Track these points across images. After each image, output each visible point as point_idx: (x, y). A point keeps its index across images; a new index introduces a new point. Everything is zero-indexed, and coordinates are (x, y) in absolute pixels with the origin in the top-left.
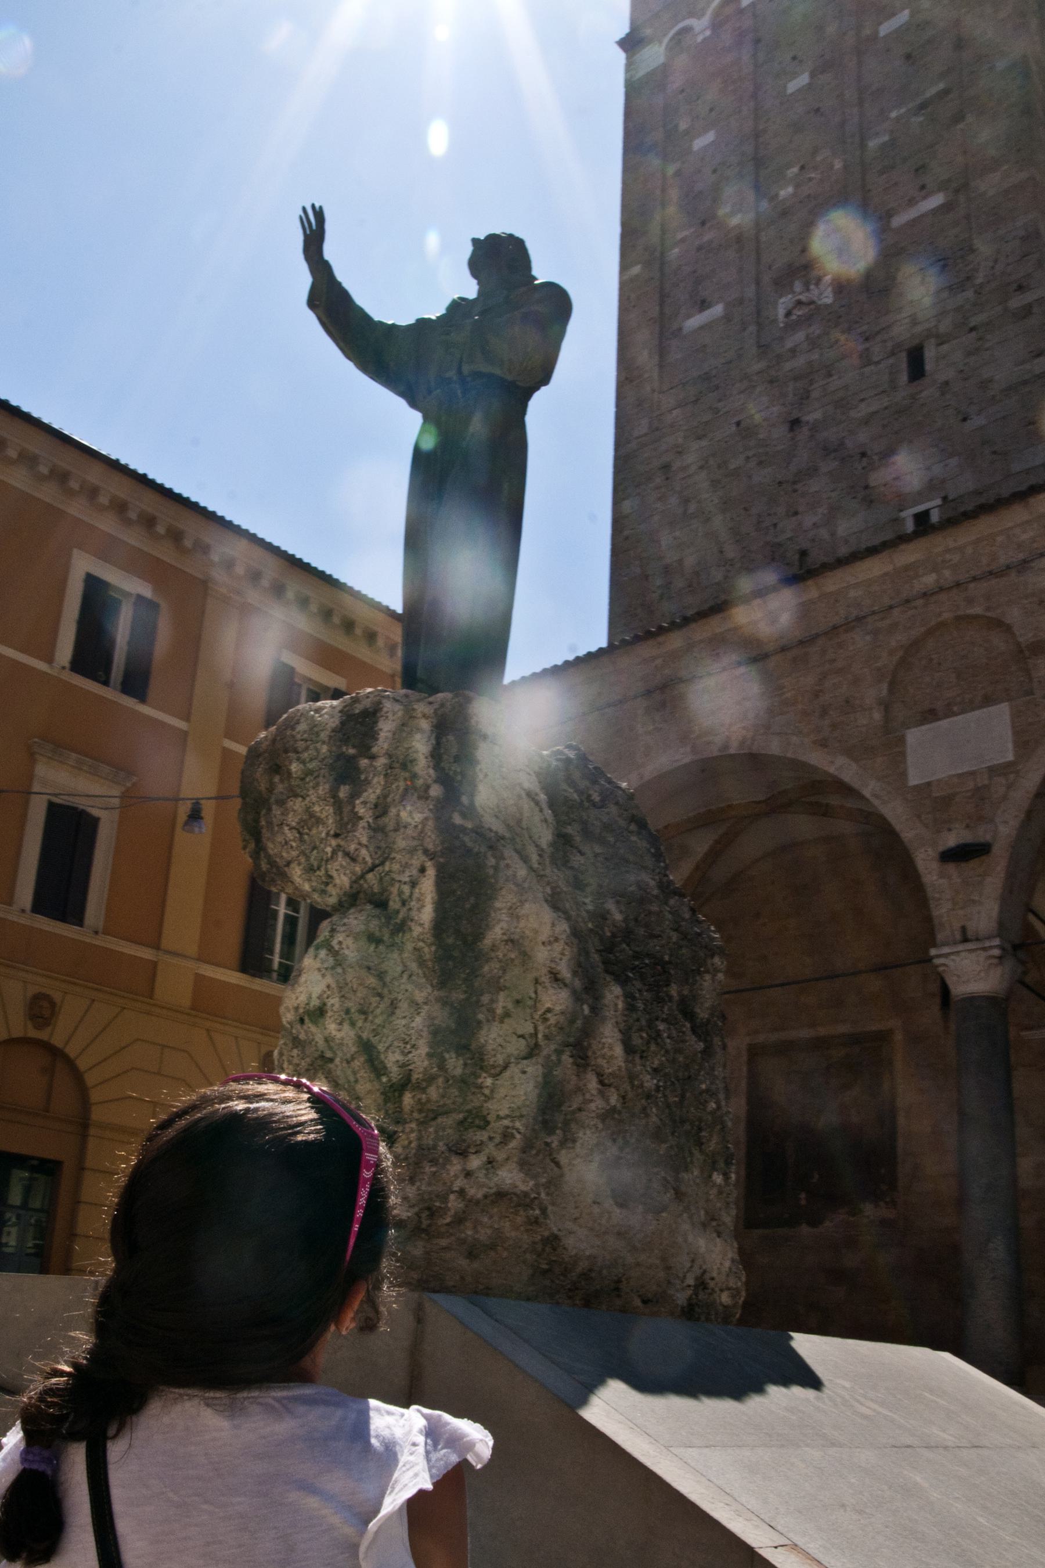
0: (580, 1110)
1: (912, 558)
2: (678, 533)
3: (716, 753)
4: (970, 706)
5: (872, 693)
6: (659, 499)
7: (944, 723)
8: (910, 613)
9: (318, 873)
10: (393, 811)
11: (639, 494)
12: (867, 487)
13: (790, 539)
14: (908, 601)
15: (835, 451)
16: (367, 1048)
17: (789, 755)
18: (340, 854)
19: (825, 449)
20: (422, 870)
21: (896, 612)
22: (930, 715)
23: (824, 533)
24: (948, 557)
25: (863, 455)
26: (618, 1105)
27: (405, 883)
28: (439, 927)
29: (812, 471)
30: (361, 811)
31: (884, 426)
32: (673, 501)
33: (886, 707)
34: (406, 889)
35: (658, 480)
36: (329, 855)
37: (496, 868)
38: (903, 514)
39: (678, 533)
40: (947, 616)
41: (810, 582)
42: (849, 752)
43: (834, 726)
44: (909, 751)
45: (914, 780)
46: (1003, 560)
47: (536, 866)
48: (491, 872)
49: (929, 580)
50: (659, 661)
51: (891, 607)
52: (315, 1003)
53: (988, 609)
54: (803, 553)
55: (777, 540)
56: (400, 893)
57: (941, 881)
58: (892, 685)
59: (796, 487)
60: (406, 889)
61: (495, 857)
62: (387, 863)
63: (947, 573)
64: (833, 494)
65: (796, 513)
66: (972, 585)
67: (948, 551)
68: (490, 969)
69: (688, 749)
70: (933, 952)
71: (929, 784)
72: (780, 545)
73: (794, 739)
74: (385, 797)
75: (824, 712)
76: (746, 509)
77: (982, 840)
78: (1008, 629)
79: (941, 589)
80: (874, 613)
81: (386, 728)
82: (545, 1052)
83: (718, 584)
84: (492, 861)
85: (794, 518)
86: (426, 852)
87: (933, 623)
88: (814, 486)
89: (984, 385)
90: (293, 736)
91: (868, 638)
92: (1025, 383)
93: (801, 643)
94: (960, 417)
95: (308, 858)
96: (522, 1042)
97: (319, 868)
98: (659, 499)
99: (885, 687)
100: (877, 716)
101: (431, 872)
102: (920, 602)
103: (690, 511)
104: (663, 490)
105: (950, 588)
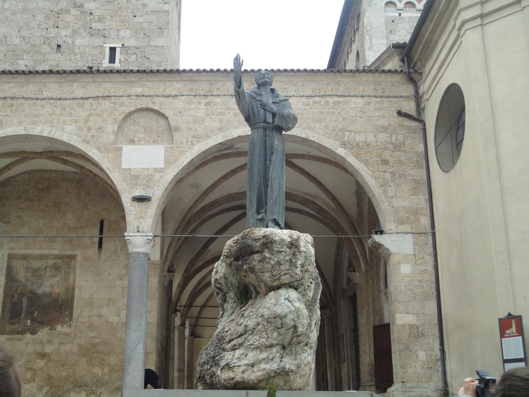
1: (133, 80)
3: (37, 134)
4: (147, 142)
5: (111, 127)
7: (138, 147)
8: (130, 101)
10: (306, 267)
12: (91, 28)
13: (54, 38)
14: (129, 96)
15: (79, 7)
16: (295, 327)
17: (71, 143)
19: (74, 4)
20: (311, 283)
21: (124, 98)
22: (132, 141)
23: (69, 40)
24: (147, 83)
25: (91, 14)
29: (67, 12)
31: (101, 5)
33: (116, 134)
38: (105, 45)
40: (144, 106)
41: (90, 75)
42: (98, 149)
43: (93, 136)
44: (123, 154)
45: (124, 166)
46: (168, 92)
49: (139, 90)
50: (12, 85)
51: (122, 96)
52: (283, 314)
53: (160, 108)
54: (59, 46)
55: (47, 36)
56: (305, 288)
57: (131, 207)
58: (119, 127)
59: (59, 16)
60: (307, 287)
63: (146, 90)
64: (77, 26)
65: (58, 27)
66: (155, 98)
67: (148, 81)
69: (23, 128)
70: (126, 234)
71: (130, 169)
72: (48, 38)
73: (74, 137)
75: (89, 129)
76: (34, 16)
77: (149, 195)
78: (166, 118)
79: (143, 96)
80: (115, 96)
83: (16, 45)
85: (56, 29)
87: (139, 107)
88: (68, 18)
89: (145, 6)
91: (112, 105)
92: (159, 11)
93: (82, 98)
94: (133, 15)
99: (116, 126)
100: (112, 137)
101: (313, 284)
102: (134, 98)
105: (147, 96)
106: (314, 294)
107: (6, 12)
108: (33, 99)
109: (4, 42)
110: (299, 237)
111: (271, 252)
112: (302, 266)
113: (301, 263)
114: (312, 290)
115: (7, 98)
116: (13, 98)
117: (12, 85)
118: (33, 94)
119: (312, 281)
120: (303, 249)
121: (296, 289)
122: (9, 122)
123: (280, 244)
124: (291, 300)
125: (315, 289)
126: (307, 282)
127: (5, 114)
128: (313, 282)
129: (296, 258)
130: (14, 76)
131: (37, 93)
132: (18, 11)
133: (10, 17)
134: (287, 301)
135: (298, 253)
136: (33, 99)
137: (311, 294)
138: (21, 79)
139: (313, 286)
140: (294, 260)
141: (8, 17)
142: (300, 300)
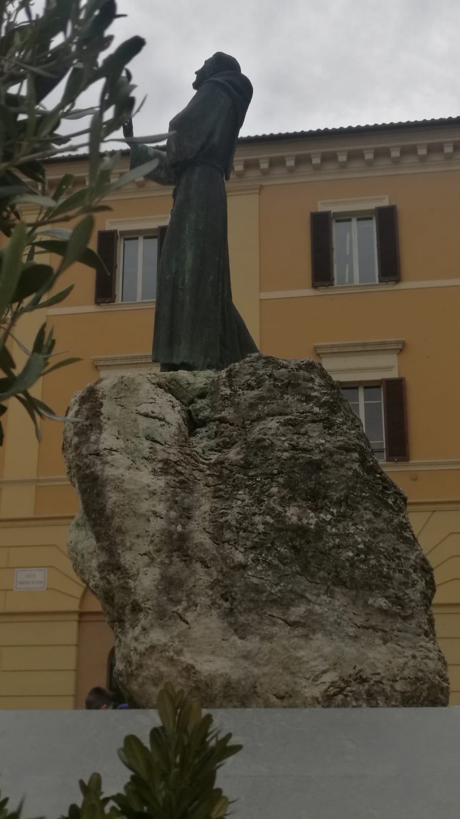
0: (194, 586)
26: (220, 577)
37: (102, 470)
48: (99, 473)
68: (116, 522)
82: (159, 560)
96: (146, 558)
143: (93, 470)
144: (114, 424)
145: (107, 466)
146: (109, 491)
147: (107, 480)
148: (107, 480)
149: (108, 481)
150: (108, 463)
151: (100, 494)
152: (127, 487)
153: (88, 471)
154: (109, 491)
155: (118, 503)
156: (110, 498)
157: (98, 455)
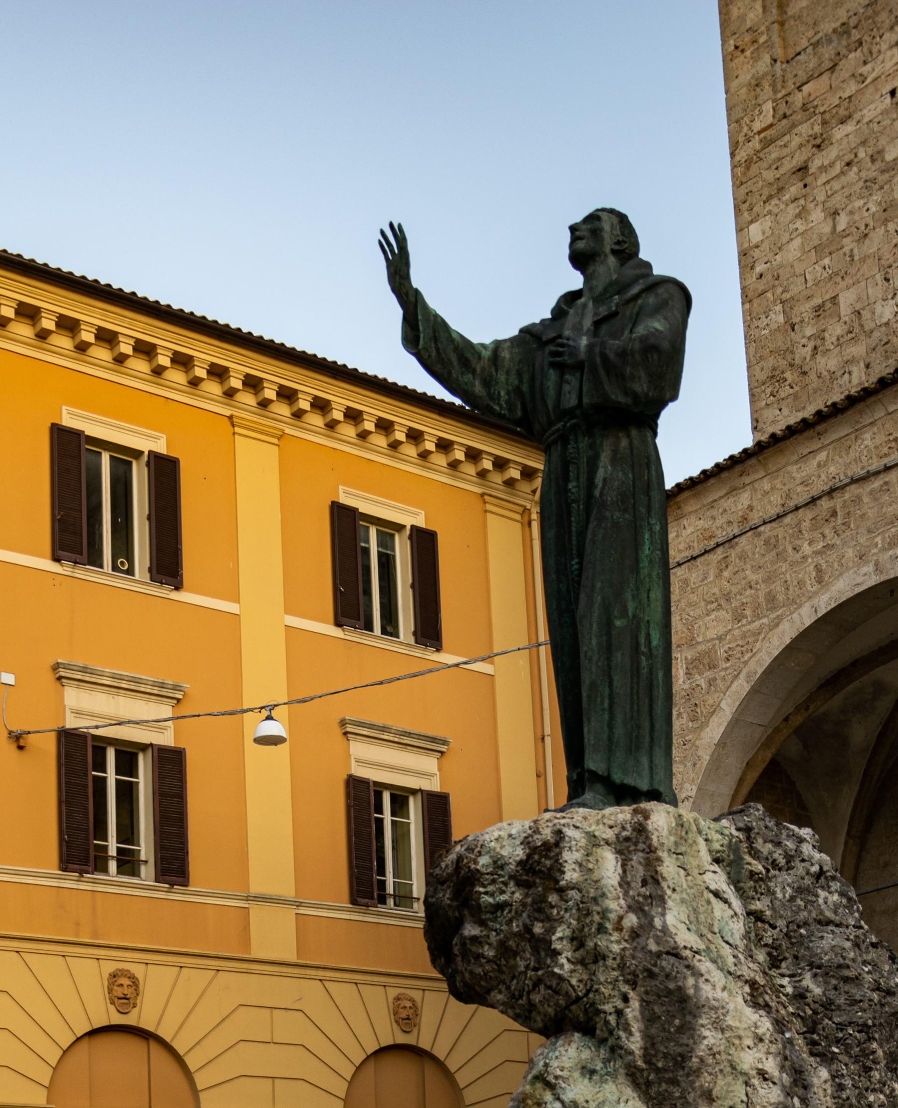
2: (826, 261)
6: (799, 216)
9: (520, 1002)
10: (590, 944)
11: (770, 212)
18: (542, 987)
20: (626, 999)
27: (610, 1014)
28: (647, 1057)
30: (557, 946)
32: (817, 215)
34: (612, 1019)
35: (794, 189)
36: (531, 987)
37: (696, 987)
39: (826, 261)
47: (732, 969)
56: (607, 1023)
60: (612, 1019)
61: (693, 975)
62: (591, 995)
74: (582, 930)
81: (570, 857)
84: (691, 981)
86: (627, 982)
90: (478, 870)
95: (508, 988)
97: (521, 997)
98: (799, 216)
101: (635, 1004)
103: (840, 228)
104: (802, 202)
106: (647, 1036)
107: (846, 241)
108: (877, 473)
109: (857, 329)
110: (560, 832)
111: (479, 914)
112: (578, 940)
113: (568, 932)
114: (635, 1027)
115: (820, 498)
116: (830, 493)
117: (822, 456)
118: (875, 459)
119: (625, 988)
120: (571, 875)
121: (587, 1029)
122: (836, 564)
123: (494, 882)
124: (551, 1079)
125: (650, 1019)
126: (607, 999)
127: (821, 544)
128: (631, 994)
129: (549, 919)
130: (819, 428)
131: (885, 450)
132: (871, 224)
133: (856, 251)
134: (539, 1085)
135: (553, 898)
136: (877, 473)
137: (635, 1043)
138: (839, 430)
139: (633, 1011)
140: (538, 929)
141: (852, 256)
142: (593, 1072)
143: (680, 984)
144: (683, 901)
145: (701, 980)
146: (703, 1026)
147: (703, 1006)
148: (703, 1006)
149: (706, 1009)
150: (702, 975)
151: (688, 1029)
152: (731, 1023)
153: (672, 986)
154: (703, 1026)
155: (715, 1050)
156: (705, 1038)
157: (677, 956)
